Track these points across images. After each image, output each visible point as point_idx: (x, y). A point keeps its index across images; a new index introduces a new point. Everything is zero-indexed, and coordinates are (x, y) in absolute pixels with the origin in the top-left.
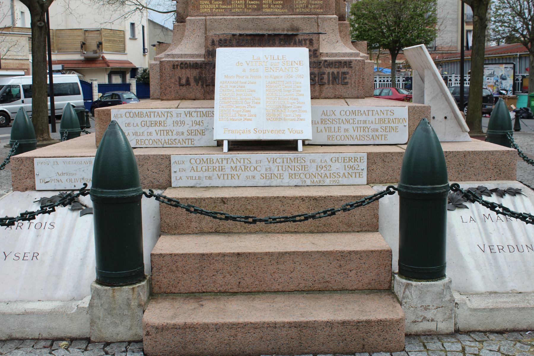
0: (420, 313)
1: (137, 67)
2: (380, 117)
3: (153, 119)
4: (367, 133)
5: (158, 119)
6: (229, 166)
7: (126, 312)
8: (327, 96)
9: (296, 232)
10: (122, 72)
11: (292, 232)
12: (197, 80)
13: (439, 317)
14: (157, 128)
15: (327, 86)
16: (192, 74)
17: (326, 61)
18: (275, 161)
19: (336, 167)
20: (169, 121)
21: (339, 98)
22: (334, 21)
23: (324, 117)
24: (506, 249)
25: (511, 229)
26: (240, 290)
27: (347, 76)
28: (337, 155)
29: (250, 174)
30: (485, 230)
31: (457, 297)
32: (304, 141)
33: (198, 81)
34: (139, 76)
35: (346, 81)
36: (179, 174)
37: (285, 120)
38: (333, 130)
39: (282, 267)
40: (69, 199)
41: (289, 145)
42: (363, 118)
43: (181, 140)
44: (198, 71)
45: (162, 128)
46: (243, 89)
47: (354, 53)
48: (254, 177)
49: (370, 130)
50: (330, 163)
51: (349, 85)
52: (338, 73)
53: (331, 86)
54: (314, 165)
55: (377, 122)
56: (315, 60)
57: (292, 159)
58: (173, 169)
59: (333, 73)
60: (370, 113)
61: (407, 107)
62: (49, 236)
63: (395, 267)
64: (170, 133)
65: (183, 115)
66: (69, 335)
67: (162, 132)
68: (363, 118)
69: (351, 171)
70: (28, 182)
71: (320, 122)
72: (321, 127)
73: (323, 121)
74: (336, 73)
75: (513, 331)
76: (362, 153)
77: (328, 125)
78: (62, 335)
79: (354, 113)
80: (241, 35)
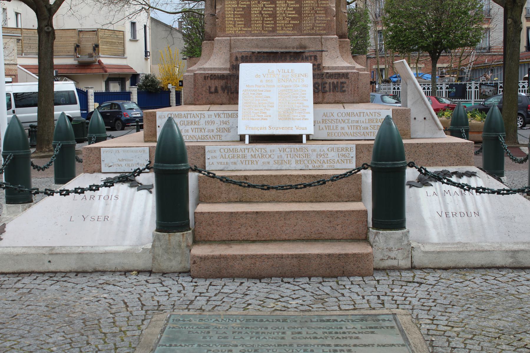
1: (138, 72)
2: (369, 118)
3: (189, 119)
4: (359, 131)
5: (193, 119)
6: (249, 154)
8: (328, 102)
9: (299, 202)
10: (120, 79)
11: (296, 202)
12: (224, 89)
14: (193, 127)
15: (328, 93)
16: (219, 84)
17: (327, 73)
18: (284, 150)
19: (332, 155)
20: (202, 121)
21: (338, 103)
22: (335, 40)
23: (324, 118)
25: (464, 201)
26: (258, 239)
27: (345, 85)
28: (333, 146)
29: (266, 160)
32: (308, 136)
33: (225, 89)
34: (140, 83)
35: (344, 89)
36: (211, 161)
37: (293, 119)
38: (331, 128)
40: (128, 179)
41: (296, 139)
42: (356, 118)
43: (211, 136)
44: (224, 81)
45: (196, 126)
46: (300, 335)
47: (351, 67)
48: (269, 163)
49: (361, 128)
50: (327, 152)
51: (346, 93)
52: (337, 83)
53: (332, 93)
54: (315, 153)
55: (367, 121)
56: (319, 72)
57: (298, 149)
58: (207, 157)
59: (333, 83)
60: (362, 114)
61: (391, 110)
62: (115, 205)
63: (370, 224)
64: (203, 131)
65: (213, 117)
66: (136, 269)
67: (197, 130)
68: (356, 118)
69: (343, 158)
70: (96, 166)
71: (321, 122)
72: (322, 125)
73: (324, 121)
74: (335, 83)
75: (454, 268)
76: (352, 145)
77: (328, 124)
78: (132, 269)
79: (348, 114)
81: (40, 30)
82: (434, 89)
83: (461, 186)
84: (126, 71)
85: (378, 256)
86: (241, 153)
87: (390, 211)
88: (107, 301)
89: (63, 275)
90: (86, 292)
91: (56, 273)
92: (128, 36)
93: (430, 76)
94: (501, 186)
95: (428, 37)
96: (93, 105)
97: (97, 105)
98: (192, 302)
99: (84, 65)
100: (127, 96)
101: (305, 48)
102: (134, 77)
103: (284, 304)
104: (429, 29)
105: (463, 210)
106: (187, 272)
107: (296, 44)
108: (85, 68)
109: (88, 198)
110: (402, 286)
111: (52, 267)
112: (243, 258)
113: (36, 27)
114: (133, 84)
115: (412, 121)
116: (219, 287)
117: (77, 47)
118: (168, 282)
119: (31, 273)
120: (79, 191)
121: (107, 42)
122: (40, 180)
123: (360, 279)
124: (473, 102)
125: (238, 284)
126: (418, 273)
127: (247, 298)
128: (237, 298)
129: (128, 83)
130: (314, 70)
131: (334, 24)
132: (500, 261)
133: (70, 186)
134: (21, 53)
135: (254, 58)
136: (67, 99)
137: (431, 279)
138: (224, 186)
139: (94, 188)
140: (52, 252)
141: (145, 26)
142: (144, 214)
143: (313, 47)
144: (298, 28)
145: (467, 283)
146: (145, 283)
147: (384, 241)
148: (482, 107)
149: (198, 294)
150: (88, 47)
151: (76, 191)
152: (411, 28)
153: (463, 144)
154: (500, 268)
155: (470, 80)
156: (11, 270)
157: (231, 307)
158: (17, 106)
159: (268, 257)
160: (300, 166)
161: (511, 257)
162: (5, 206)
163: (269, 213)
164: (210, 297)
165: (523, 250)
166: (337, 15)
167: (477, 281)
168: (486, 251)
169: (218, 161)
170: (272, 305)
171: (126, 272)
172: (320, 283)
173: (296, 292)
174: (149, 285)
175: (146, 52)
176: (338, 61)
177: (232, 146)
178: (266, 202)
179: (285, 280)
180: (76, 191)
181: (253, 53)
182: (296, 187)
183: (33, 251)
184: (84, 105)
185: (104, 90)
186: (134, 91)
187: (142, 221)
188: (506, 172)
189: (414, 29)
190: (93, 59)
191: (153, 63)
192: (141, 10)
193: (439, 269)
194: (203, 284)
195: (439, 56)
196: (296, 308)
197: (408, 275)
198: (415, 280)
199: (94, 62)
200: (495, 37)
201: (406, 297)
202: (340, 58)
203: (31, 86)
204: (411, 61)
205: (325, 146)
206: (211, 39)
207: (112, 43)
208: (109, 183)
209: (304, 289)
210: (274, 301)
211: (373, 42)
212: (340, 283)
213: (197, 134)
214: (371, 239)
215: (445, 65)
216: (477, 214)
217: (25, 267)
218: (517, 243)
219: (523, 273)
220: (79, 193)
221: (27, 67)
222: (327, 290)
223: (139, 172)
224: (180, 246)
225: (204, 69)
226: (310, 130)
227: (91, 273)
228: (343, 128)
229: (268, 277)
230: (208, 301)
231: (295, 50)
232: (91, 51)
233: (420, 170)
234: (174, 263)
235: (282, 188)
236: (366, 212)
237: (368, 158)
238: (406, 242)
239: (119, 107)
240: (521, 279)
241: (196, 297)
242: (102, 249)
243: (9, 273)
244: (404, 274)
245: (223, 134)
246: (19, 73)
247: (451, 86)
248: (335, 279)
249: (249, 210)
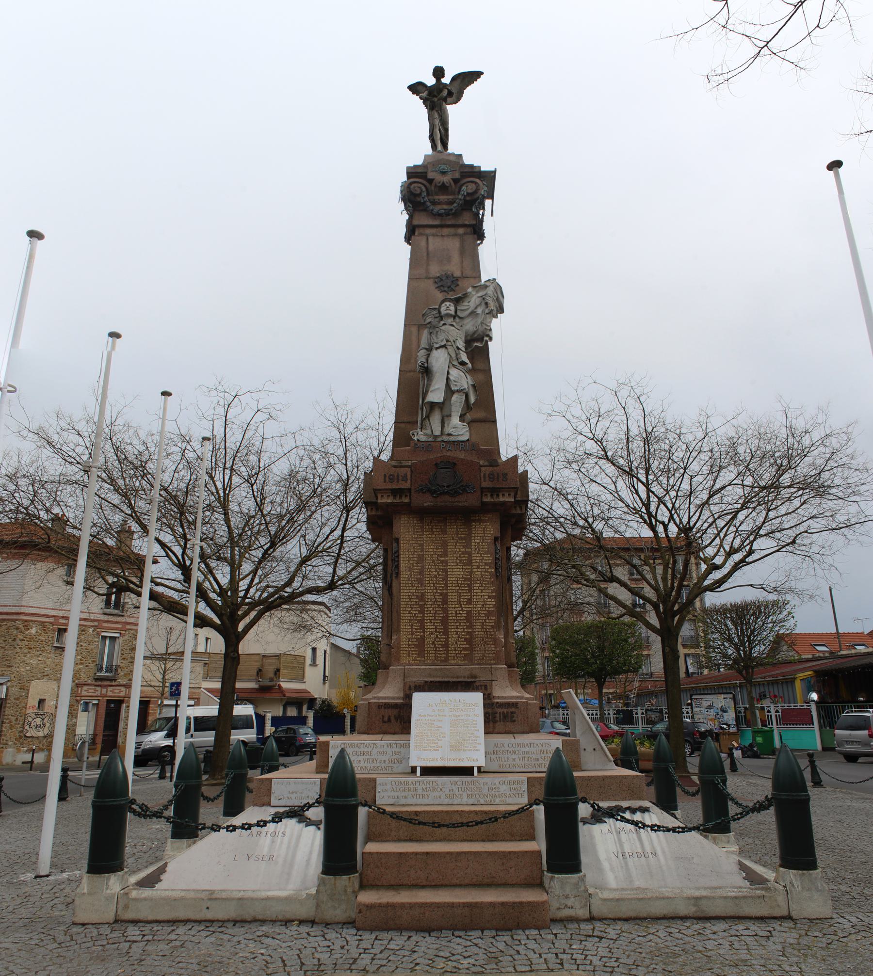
0: (563, 902)
3: (362, 749)
5: (366, 750)
7: (343, 897)
9: (471, 841)
11: (468, 841)
12: (397, 718)
13: (577, 905)
14: (365, 757)
16: (393, 712)
18: (456, 783)
19: (504, 788)
20: (375, 751)
24: (635, 855)
26: (428, 883)
28: (504, 779)
29: (436, 794)
30: (619, 839)
31: (591, 891)
32: (479, 768)
33: (397, 719)
36: (382, 794)
37: (464, 750)
39: (459, 864)
40: (297, 813)
41: (467, 771)
42: (527, 749)
44: (397, 710)
45: (368, 757)
48: (440, 797)
54: (486, 787)
56: (489, 702)
62: (282, 842)
63: (545, 867)
65: (385, 747)
66: (298, 918)
68: (527, 749)
69: (515, 792)
70: (266, 799)
72: (493, 757)
73: (495, 752)
75: (636, 918)
76: (524, 778)
78: (293, 918)
79: (519, 745)
80: (431, 682)
81: (226, 655)
82: (602, 715)
83: (635, 824)
84: (305, 695)
85: (555, 904)
86: (412, 786)
87: (565, 855)
88: (264, 957)
89: (220, 924)
90: (242, 946)
91: (212, 921)
92: (308, 661)
93: (597, 702)
94: (676, 823)
95: (593, 663)
96: (269, 730)
97: (273, 729)
98: (355, 960)
99: (264, 689)
100: (302, 721)
101: (476, 677)
102: (312, 701)
103: (455, 964)
104: (593, 656)
105: (640, 850)
106: (350, 923)
107: (467, 673)
108: (266, 691)
109: (255, 833)
110: (581, 941)
111: (209, 915)
112: (412, 906)
113: (223, 652)
114: (309, 708)
115: (582, 751)
116: (385, 942)
117: (260, 671)
118: (331, 935)
119: (186, 921)
120: (247, 827)
121: (288, 667)
122: (209, 812)
123: (536, 932)
124: (640, 728)
125: (406, 938)
126: (598, 924)
127: (415, 956)
128: (404, 956)
129: (305, 707)
130: (484, 699)
131: (503, 654)
132: (683, 910)
133: (238, 821)
134: (207, 677)
135: (426, 688)
136: (245, 723)
137: (612, 932)
138: (394, 823)
139: (262, 824)
140: (212, 897)
141: (325, 651)
142: (311, 853)
143: (483, 677)
144: (469, 658)
145: (650, 937)
146: (305, 935)
147: (560, 885)
148: (650, 733)
149: (362, 951)
150: (269, 671)
151: (243, 827)
152: (577, 655)
153: (634, 777)
154: (684, 918)
155: (636, 706)
156: (166, 918)
157: (397, 967)
158: (195, 730)
159: (438, 905)
160: (471, 801)
161: (695, 905)
162: (170, 840)
163: (439, 853)
164: (375, 955)
165: (705, 897)
166: (505, 646)
167: (660, 934)
168: (668, 898)
169: (390, 794)
170: (442, 965)
171: (287, 922)
172: (494, 937)
173: (468, 949)
174: (310, 939)
175: (324, 676)
176: (508, 691)
177: (403, 779)
178: (436, 841)
179: (457, 933)
180: (243, 827)
181: (426, 682)
182: (467, 825)
183: (192, 895)
184: (261, 730)
185: (281, 714)
186: (311, 715)
187: (308, 861)
188: (680, 804)
189: (579, 655)
190: (273, 683)
191: (331, 687)
192: (321, 638)
193: (620, 919)
194: (369, 937)
195: (605, 681)
196: (467, 969)
197: (586, 927)
198: (595, 934)
199: (274, 686)
200: (656, 663)
201: (587, 956)
202: (510, 688)
203: (211, 710)
204: (579, 691)
205: (497, 779)
206: (386, 667)
207: (292, 668)
208: (277, 818)
209: (476, 945)
210: (444, 960)
211: (541, 668)
212: (515, 937)
213: (369, 765)
214: (546, 885)
215: (611, 691)
216: (655, 854)
217: (181, 914)
218: (698, 889)
219: (708, 925)
220: (246, 829)
221: (211, 691)
222: (501, 946)
223: (309, 806)
224: (346, 891)
225: (379, 698)
226: (482, 763)
227: (250, 922)
228: (514, 760)
229: (437, 930)
230: (373, 959)
231: (466, 680)
232: (272, 675)
233: (592, 806)
234: (338, 912)
235: (454, 826)
236: (539, 852)
237: (540, 793)
238: (583, 888)
239: (295, 731)
240: (708, 932)
241: (360, 954)
242: (264, 894)
243: (164, 922)
244: (583, 926)
245: (395, 766)
246: (202, 697)
247: (618, 712)
248: (509, 933)
249: (419, 851)
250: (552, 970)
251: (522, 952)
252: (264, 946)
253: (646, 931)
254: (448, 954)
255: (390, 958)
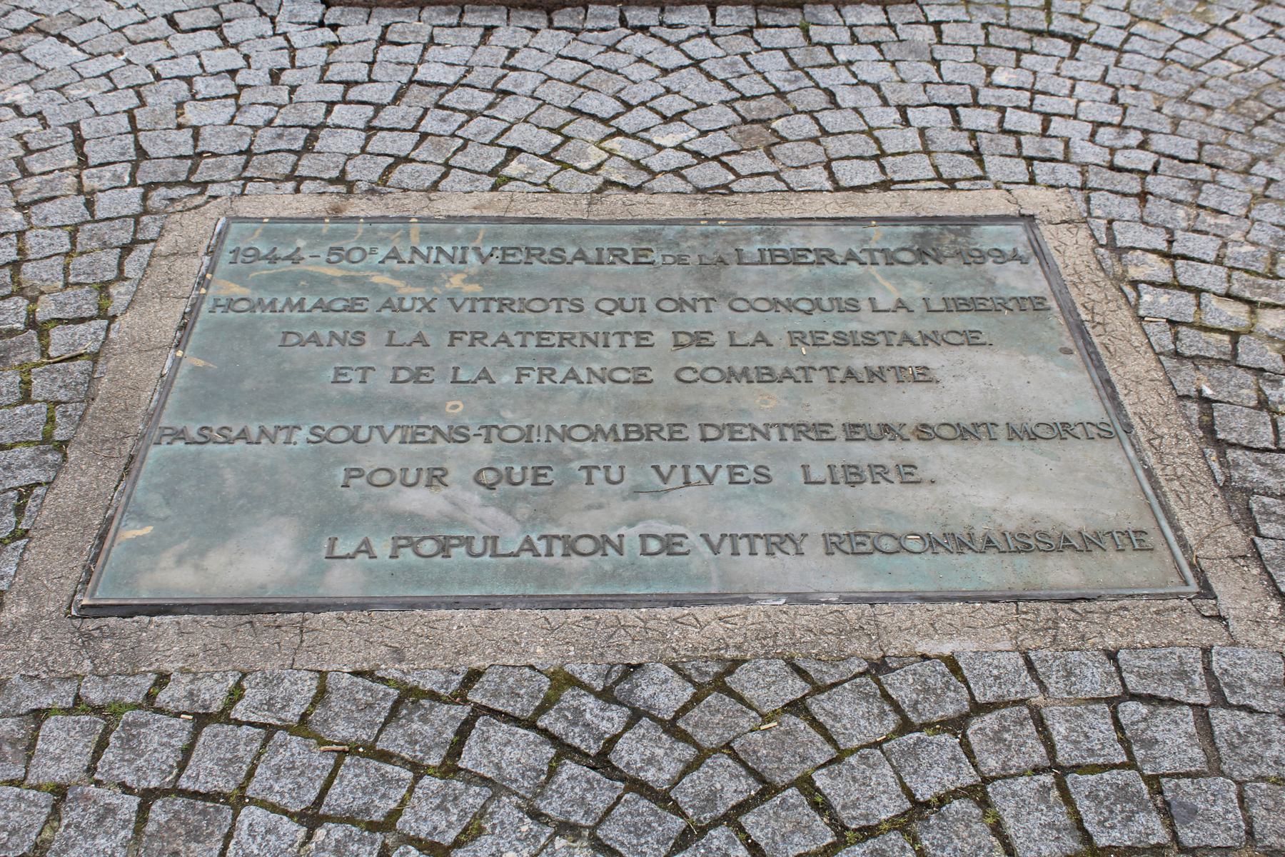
88: (20, 126)
98: (314, 132)
103: (634, 149)
110: (1019, 52)
116: (411, 53)
127: (509, 110)
128: (472, 115)
145: (1220, 39)
149: (336, 92)
157: (448, 167)
164: (379, 107)
170: (595, 156)
172: (749, 32)
173: (672, 81)
179: (636, 15)
196: (677, 172)
209: (696, 63)
210: (602, 130)
212: (816, 33)
222: (774, 65)
230: (370, 130)
241: (331, 105)
248: (794, 16)
250: (952, 183)
251: (846, 97)
252: (30, 71)
253: (1203, 17)
254: (611, 107)
255: (427, 126)
